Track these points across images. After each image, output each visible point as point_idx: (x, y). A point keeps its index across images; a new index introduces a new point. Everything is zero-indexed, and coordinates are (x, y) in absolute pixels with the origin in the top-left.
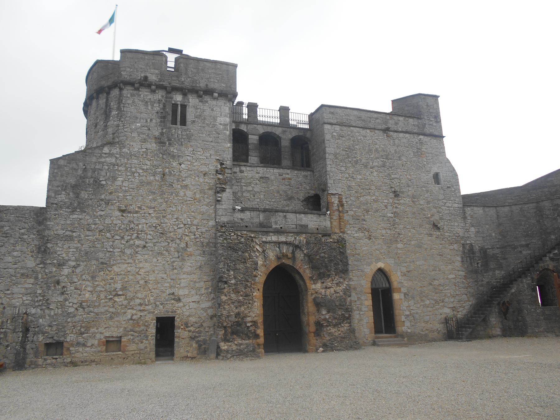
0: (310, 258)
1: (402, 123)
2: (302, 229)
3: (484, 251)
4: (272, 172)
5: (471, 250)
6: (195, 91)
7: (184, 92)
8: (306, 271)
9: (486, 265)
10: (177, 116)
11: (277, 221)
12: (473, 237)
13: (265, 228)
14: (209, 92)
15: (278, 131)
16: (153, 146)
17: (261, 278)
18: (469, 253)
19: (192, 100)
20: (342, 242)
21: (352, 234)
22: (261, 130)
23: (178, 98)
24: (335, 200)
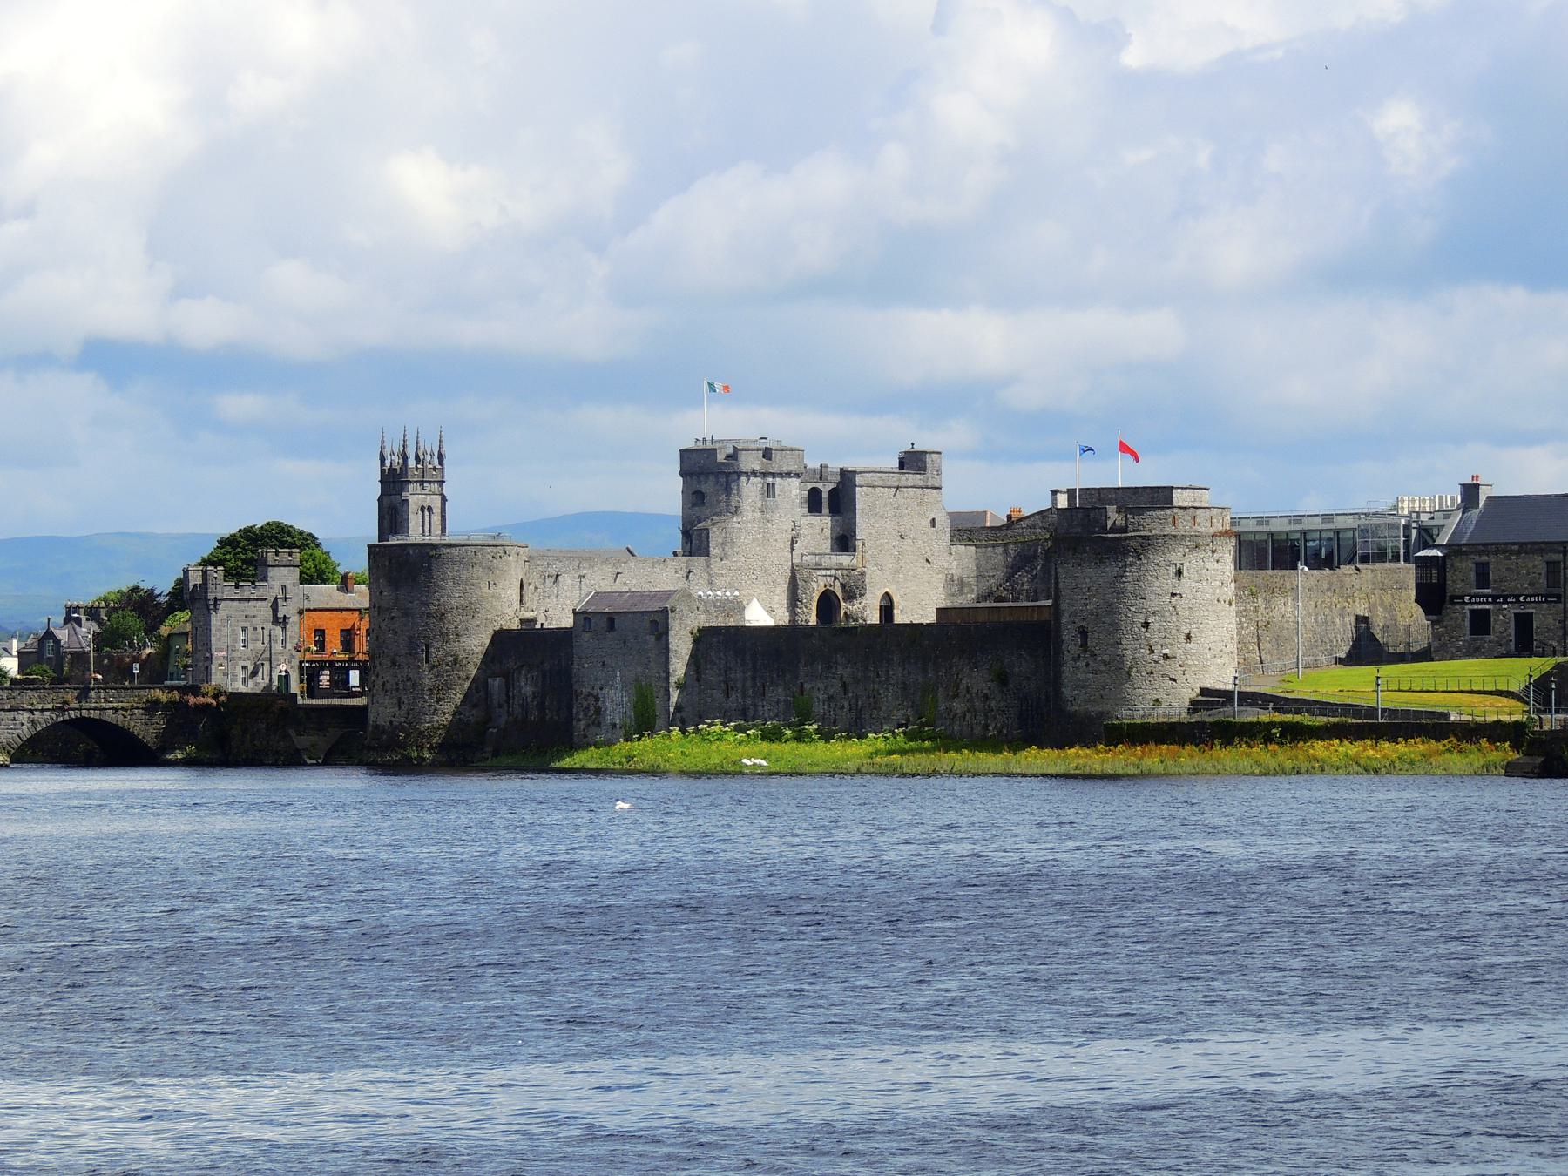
0: (843, 585)
1: (912, 478)
2: (840, 567)
3: (961, 580)
4: (815, 519)
5: (952, 579)
6: (781, 475)
7: (774, 475)
8: (839, 592)
9: (961, 591)
10: (770, 490)
11: (826, 562)
12: (955, 569)
13: (818, 567)
14: (789, 475)
15: (820, 486)
16: (758, 514)
17: (816, 599)
18: (950, 580)
19: (778, 480)
20: (863, 574)
21: (870, 569)
22: (810, 486)
23: (770, 480)
24: (859, 544)
